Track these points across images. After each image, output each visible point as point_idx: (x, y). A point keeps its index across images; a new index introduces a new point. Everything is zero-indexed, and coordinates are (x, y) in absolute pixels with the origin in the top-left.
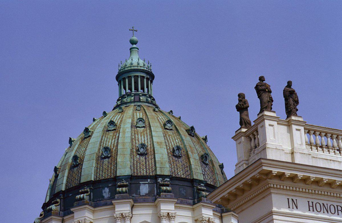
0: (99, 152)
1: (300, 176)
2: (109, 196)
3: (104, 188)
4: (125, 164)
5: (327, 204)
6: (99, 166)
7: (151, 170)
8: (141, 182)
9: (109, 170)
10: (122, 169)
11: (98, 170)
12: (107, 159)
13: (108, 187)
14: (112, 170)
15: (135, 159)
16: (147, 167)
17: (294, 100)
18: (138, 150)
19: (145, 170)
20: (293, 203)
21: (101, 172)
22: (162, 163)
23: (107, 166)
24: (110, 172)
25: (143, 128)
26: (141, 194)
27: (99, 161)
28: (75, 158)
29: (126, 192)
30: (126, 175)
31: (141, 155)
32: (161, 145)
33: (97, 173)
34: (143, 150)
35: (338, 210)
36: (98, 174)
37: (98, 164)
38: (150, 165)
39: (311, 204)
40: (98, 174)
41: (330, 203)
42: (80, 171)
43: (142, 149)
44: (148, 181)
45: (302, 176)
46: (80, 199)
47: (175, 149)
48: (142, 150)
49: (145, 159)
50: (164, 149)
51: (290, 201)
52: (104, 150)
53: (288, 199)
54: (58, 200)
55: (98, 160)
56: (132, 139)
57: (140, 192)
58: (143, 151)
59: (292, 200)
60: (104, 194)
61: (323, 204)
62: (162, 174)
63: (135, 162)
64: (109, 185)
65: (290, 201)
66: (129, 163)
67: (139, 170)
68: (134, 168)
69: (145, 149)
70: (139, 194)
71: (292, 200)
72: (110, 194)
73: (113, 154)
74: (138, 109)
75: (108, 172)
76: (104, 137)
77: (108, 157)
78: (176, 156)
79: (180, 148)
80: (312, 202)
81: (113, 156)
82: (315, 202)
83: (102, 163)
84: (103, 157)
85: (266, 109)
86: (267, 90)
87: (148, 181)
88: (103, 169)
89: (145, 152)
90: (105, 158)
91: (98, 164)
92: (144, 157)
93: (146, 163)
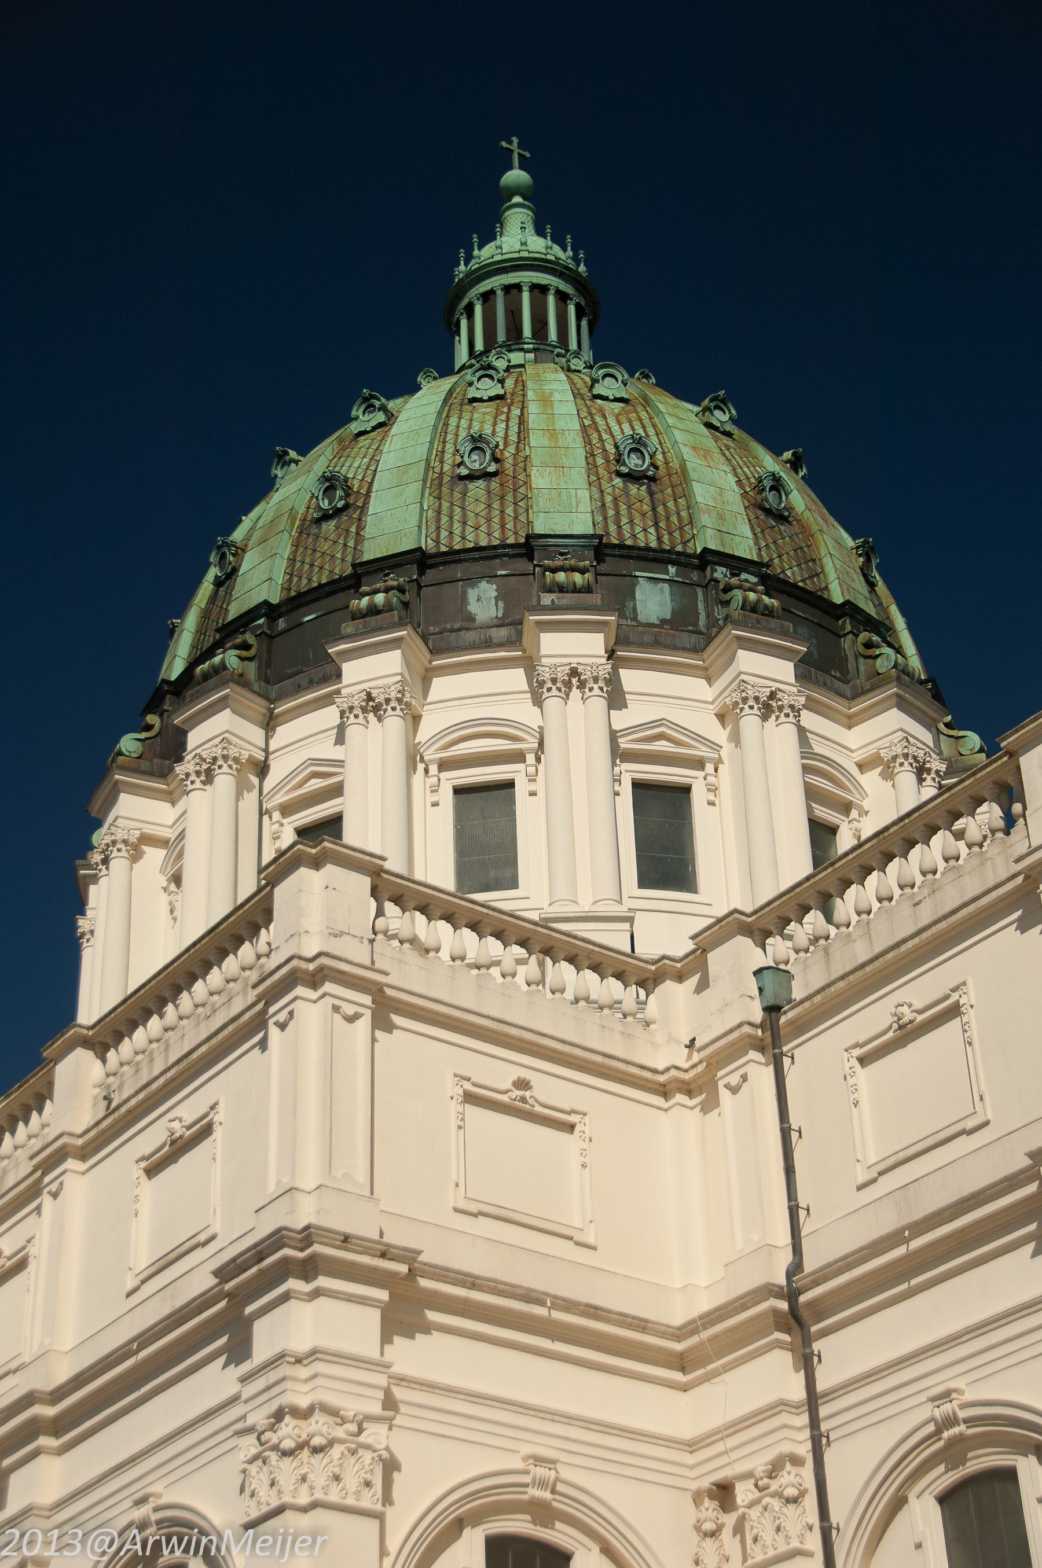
0: (442, 462)
2: (500, 615)
3: (471, 581)
4: (569, 496)
6: (445, 505)
7: (677, 534)
8: (637, 574)
9: (496, 520)
10: (555, 515)
11: (444, 519)
12: (481, 483)
13: (492, 577)
14: (508, 519)
15: (608, 490)
16: (662, 524)
18: (619, 460)
19: (652, 530)
21: (457, 525)
22: (721, 517)
23: (483, 506)
24: (497, 527)
25: (622, 405)
26: (641, 618)
27: (445, 490)
28: (330, 483)
29: (588, 589)
30: (575, 532)
31: (632, 477)
32: (709, 458)
33: (438, 528)
34: (640, 462)
36: (444, 534)
37: (440, 499)
38: (674, 519)
40: (444, 534)
42: (353, 529)
43: (632, 455)
44: (667, 573)
46: (373, 611)
47: (767, 483)
48: (633, 462)
49: (651, 494)
50: (723, 473)
52: (468, 449)
54: (249, 638)
55: (440, 485)
56: (584, 428)
57: (635, 609)
58: (636, 465)
60: (473, 607)
62: (727, 551)
63: (609, 499)
64: (499, 573)
66: (584, 494)
67: (626, 528)
68: (605, 518)
69: (647, 457)
70: (635, 618)
72: (501, 604)
73: (507, 466)
74: (573, 367)
75: (489, 527)
76: (453, 421)
77: (487, 475)
78: (768, 512)
79: (782, 486)
81: (510, 472)
83: (457, 495)
84: (464, 471)
87: (667, 573)
88: (464, 515)
89: (647, 469)
90: (471, 477)
91: (440, 499)
92: (644, 488)
93: (654, 509)
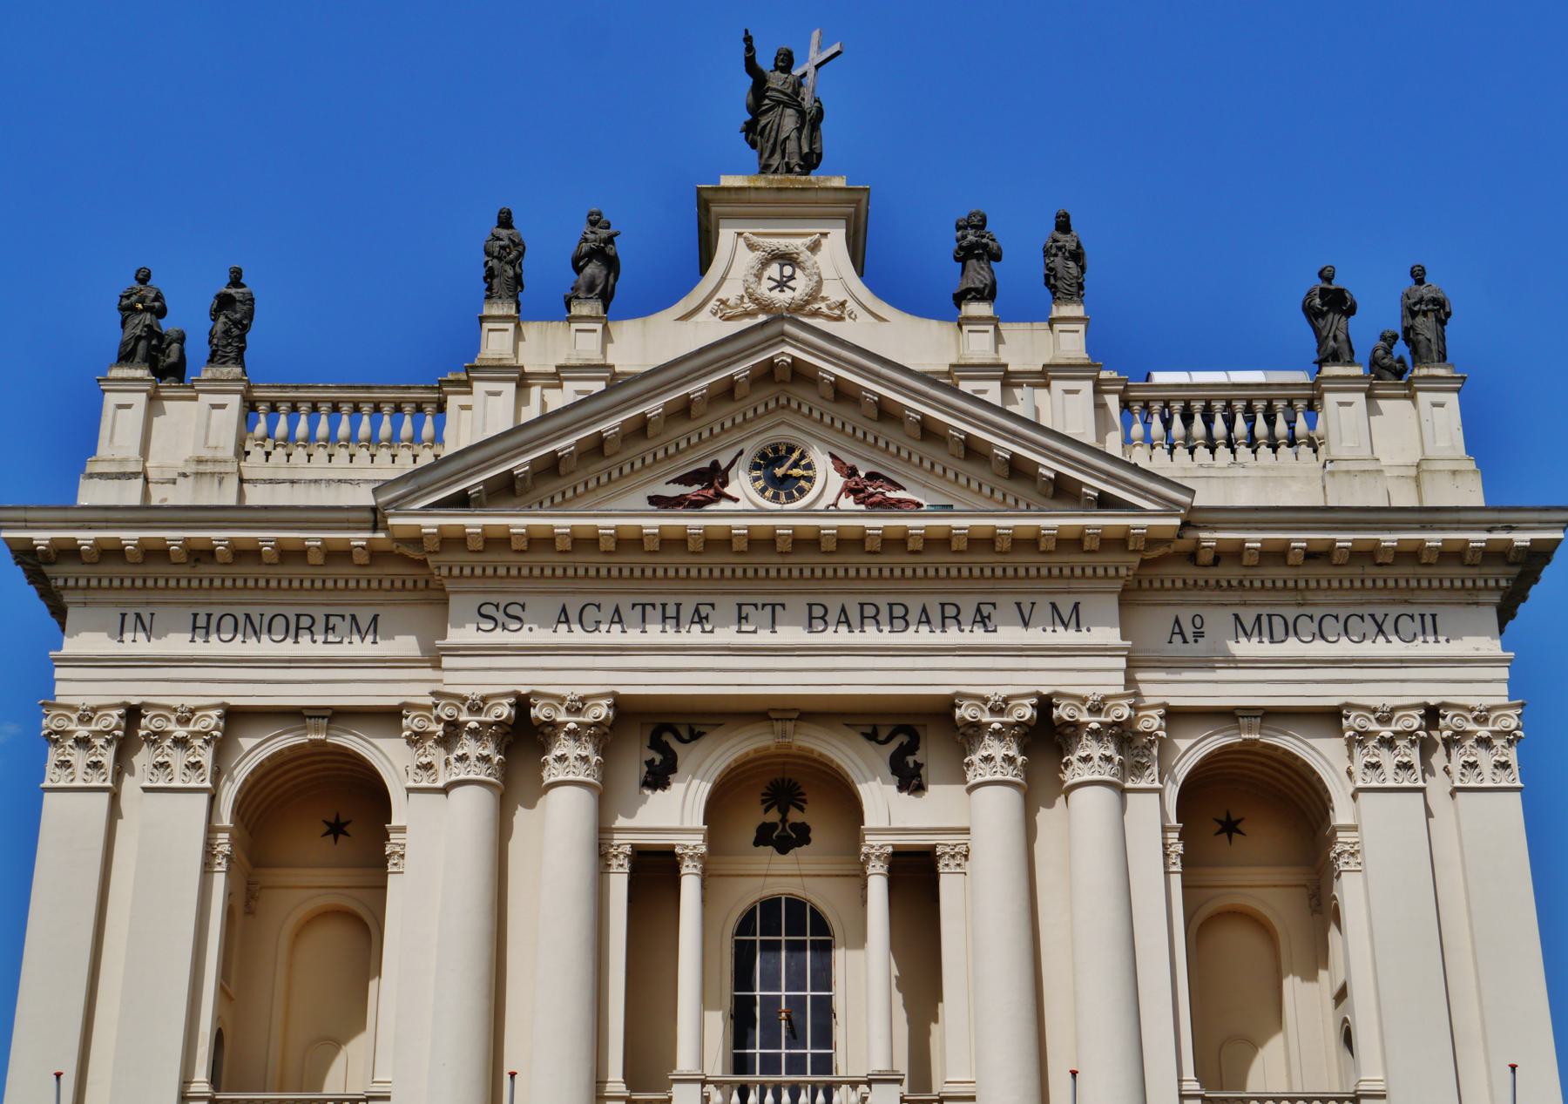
1: (85, 542)
5: (262, 615)
17: (230, 320)
20: (1238, 624)
35: (298, 628)
39: (201, 621)
41: (269, 612)
45: (136, 542)
51: (130, 620)
53: (123, 615)
59: (138, 616)
61: (248, 616)
65: (130, 620)
71: (138, 616)
80: (209, 616)
82: (217, 612)
85: (127, 362)
86: (140, 306)
